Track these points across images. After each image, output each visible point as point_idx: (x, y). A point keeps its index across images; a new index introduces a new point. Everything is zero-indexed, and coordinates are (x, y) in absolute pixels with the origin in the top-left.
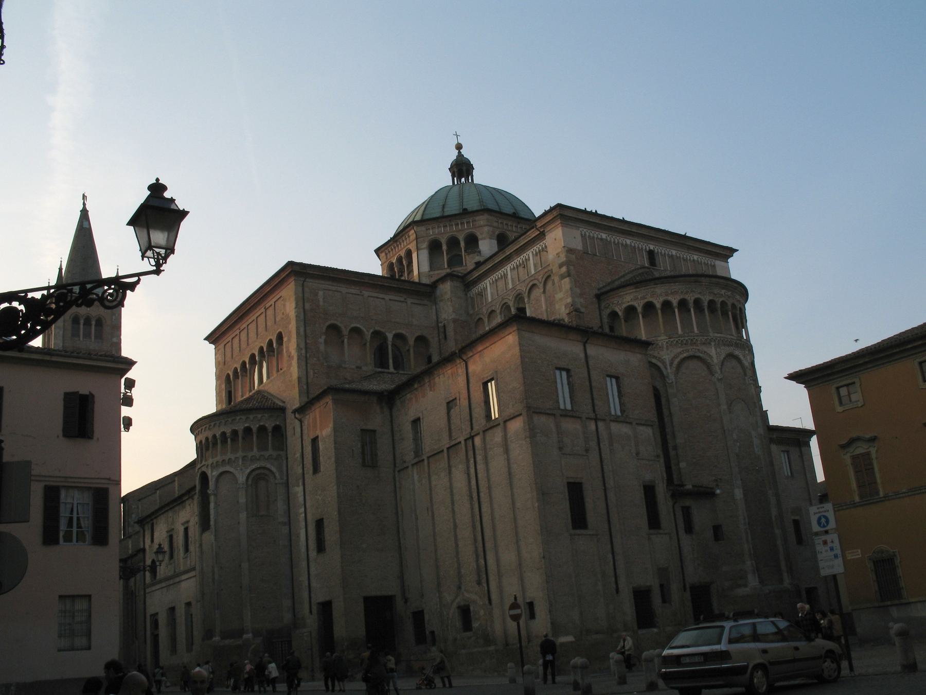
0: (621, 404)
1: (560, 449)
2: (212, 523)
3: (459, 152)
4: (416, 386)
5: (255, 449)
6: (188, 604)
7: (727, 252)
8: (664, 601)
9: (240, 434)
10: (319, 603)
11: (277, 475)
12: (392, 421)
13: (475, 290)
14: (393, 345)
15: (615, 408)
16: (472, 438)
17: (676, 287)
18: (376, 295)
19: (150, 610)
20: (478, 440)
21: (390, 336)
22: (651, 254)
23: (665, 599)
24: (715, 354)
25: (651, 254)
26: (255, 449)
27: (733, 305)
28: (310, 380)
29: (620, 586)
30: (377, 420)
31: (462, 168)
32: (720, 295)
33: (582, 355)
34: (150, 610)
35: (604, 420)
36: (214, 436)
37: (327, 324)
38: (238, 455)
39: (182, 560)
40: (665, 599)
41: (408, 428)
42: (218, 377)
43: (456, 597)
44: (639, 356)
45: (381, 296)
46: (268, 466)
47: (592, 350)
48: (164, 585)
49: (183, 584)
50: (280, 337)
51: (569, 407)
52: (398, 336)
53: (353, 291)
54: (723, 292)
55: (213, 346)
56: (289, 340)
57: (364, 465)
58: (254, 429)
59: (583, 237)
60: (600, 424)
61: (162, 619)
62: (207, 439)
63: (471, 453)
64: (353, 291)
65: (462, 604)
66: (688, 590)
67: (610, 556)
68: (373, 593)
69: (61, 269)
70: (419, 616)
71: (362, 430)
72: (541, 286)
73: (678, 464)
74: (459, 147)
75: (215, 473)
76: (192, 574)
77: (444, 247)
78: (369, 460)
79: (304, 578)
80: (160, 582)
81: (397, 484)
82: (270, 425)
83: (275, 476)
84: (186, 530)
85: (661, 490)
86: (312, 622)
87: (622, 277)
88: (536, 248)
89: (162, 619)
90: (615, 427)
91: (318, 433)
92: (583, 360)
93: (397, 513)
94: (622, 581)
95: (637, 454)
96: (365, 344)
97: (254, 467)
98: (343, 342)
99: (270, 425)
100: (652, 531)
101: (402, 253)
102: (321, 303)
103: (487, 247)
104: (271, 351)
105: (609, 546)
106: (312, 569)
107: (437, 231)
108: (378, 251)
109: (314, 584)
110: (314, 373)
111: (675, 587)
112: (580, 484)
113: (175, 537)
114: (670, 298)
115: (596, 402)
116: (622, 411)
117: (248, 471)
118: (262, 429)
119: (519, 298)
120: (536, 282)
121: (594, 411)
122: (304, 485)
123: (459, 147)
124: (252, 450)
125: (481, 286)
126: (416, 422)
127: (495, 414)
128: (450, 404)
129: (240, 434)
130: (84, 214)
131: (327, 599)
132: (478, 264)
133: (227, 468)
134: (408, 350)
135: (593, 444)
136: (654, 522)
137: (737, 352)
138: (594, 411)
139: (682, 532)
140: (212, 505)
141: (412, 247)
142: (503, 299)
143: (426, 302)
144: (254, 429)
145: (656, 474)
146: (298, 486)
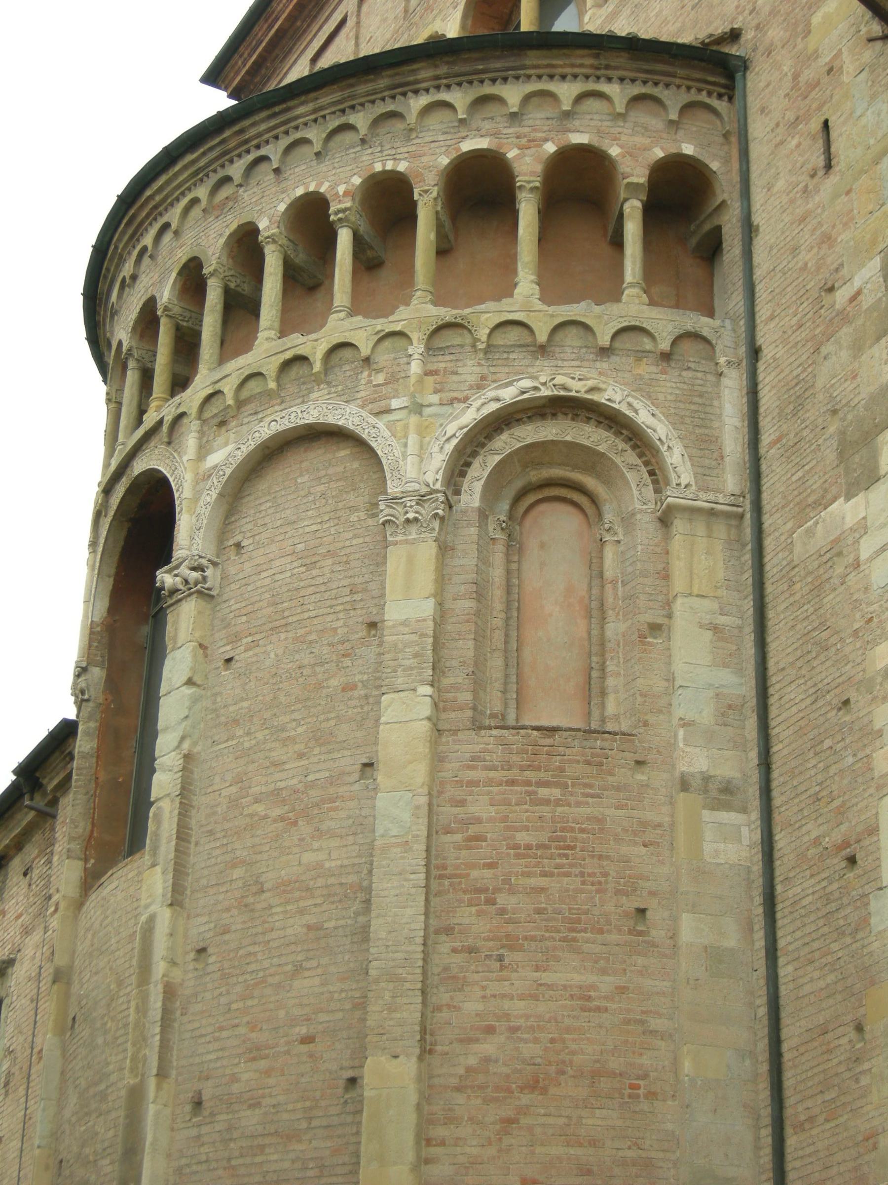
2: (164, 783)
5: (526, 283)
11: (676, 458)
26: (526, 283)
38: (400, 319)
46: (614, 395)
58: (528, 166)
75: (227, 453)
83: (656, 474)
97: (509, 395)
117: (470, 416)
118: (580, 184)
124: (507, 290)
133: (316, 410)
140: (177, 666)
144: (528, 166)
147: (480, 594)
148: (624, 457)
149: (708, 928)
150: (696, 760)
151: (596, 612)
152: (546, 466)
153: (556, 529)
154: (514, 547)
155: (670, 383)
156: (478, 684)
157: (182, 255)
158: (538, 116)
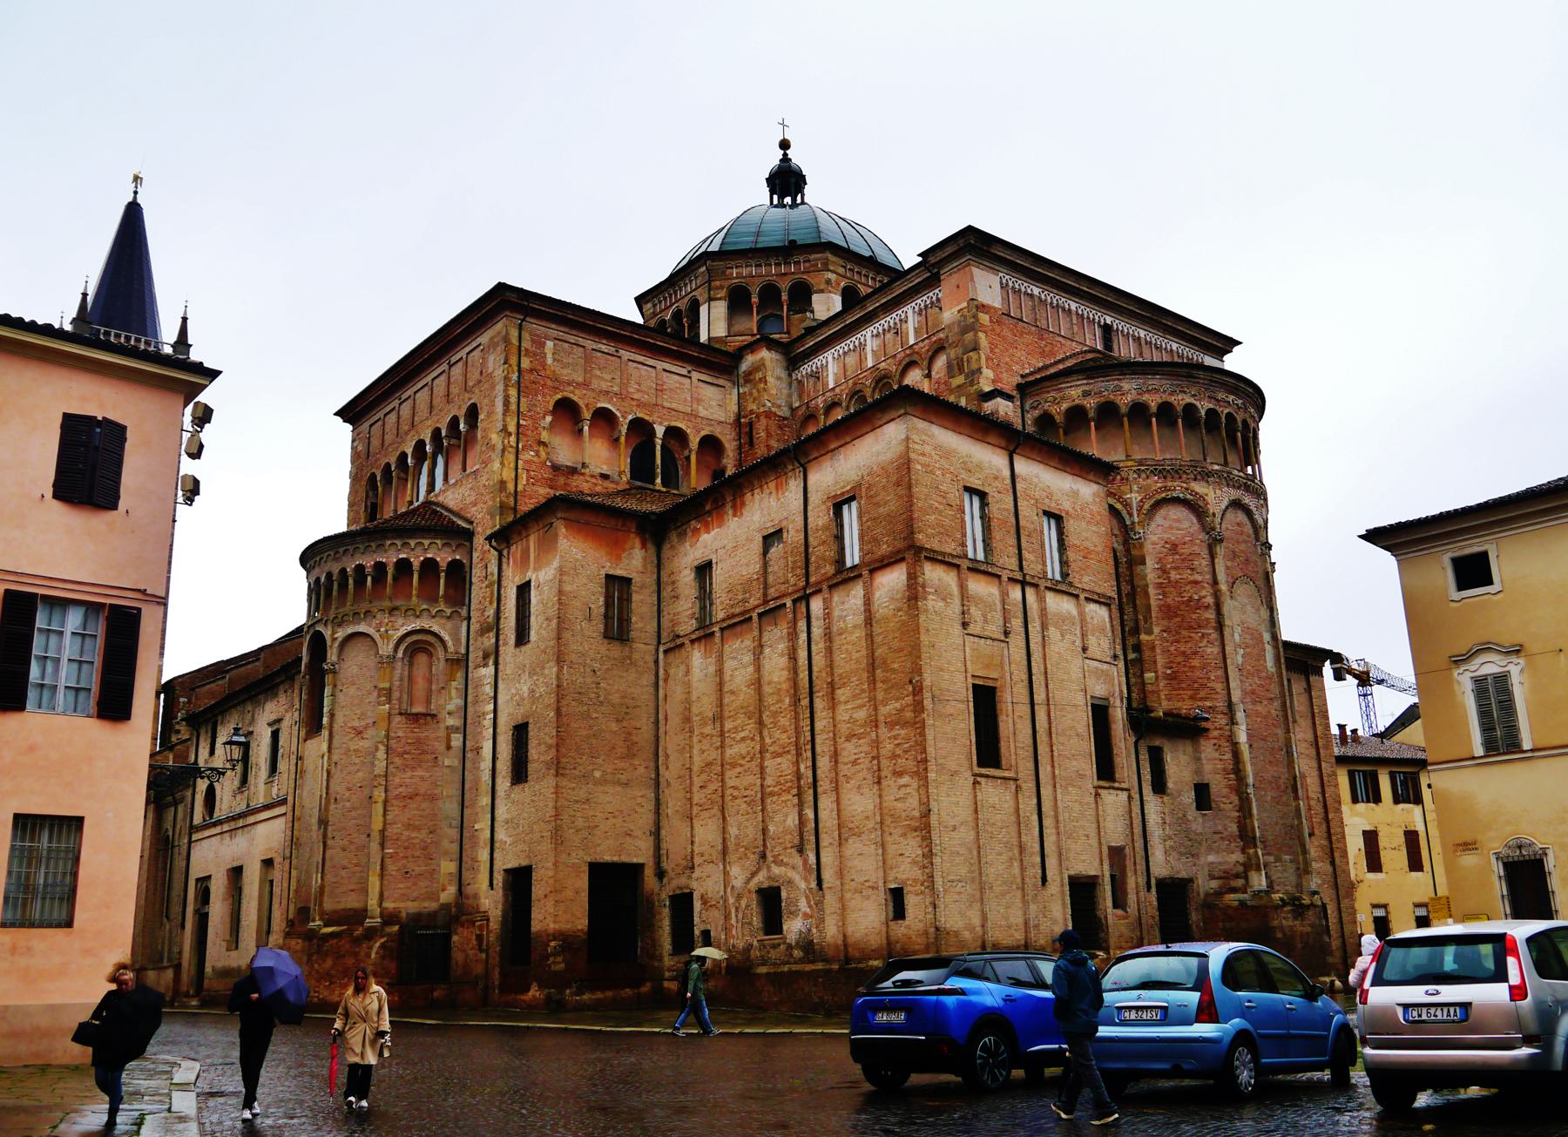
0: (1064, 563)
1: (965, 625)
3: (785, 155)
4: (708, 507)
6: (268, 863)
7: (1226, 344)
8: (1115, 906)
9: (390, 571)
10: (506, 871)
11: (450, 644)
12: (659, 566)
13: (806, 369)
14: (663, 446)
15: (1054, 570)
16: (806, 598)
17: (1154, 382)
18: (641, 359)
19: (196, 872)
20: (816, 605)
21: (660, 431)
22: (1107, 330)
23: (1119, 902)
24: (1216, 497)
25: (1107, 330)
27: (1245, 422)
28: (520, 488)
29: (1049, 874)
30: (634, 561)
31: (786, 181)
32: (1228, 404)
33: (1006, 473)
34: (196, 872)
35: (1036, 586)
36: (343, 571)
37: (559, 396)
39: (262, 787)
40: (1119, 902)
41: (687, 578)
42: (355, 478)
43: (753, 874)
44: (1094, 487)
45: (651, 362)
46: (435, 628)
47: (1023, 466)
48: (226, 827)
49: (260, 827)
50: (473, 413)
51: (981, 556)
52: (674, 433)
53: (604, 348)
54: (1231, 398)
55: (349, 427)
56: (489, 414)
57: (607, 635)
58: (416, 564)
59: (1003, 287)
60: (1030, 592)
61: (218, 887)
63: (802, 625)
64: (604, 348)
65: (765, 885)
66: (1154, 889)
67: (1035, 817)
68: (608, 858)
69: (85, 295)
70: (682, 903)
71: (608, 576)
73: (1142, 676)
74: (785, 145)
75: (340, 634)
76: (281, 810)
77: (755, 299)
78: (617, 627)
79: (483, 825)
80: (220, 822)
81: (661, 672)
82: (444, 557)
84: (275, 736)
85: (1119, 714)
86: (491, 901)
87: (1059, 362)
88: (921, 301)
89: (218, 887)
90: (1052, 600)
91: (531, 575)
92: (1008, 481)
93: (657, 722)
94: (1051, 863)
95: (1084, 649)
96: (617, 440)
98: (581, 431)
99: (444, 557)
100: (1102, 783)
102: (549, 361)
103: (827, 304)
105: (1035, 801)
106: (501, 812)
107: (745, 272)
109: (501, 835)
111: (1133, 881)
112: (993, 689)
113: (253, 745)
114: (1146, 397)
115: (1025, 554)
116: (1065, 575)
118: (430, 566)
120: (916, 358)
121: (1021, 568)
122: (496, 664)
123: (785, 145)
125: (817, 362)
127: (853, 556)
129: (390, 571)
131: (524, 863)
132: (810, 331)
133: (362, 628)
134: (688, 458)
135: (1016, 624)
136: (1106, 769)
137: (1247, 500)
138: (1021, 568)
139: (1147, 789)
141: (701, 294)
142: (855, 384)
143: (721, 382)
144: (416, 564)
145: (1110, 683)
146: (485, 665)
147: (401, 680)
148: (438, 644)
149: (451, 760)
150: (451, 722)
151: (430, 682)
152: (419, 646)
153: (422, 659)
154: (411, 665)
155: (449, 625)
156: (400, 699)
157: (327, 569)
158: (419, 550)
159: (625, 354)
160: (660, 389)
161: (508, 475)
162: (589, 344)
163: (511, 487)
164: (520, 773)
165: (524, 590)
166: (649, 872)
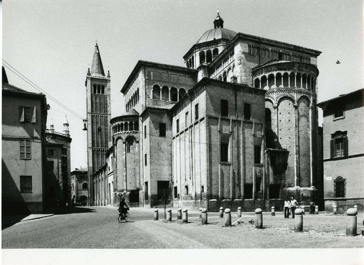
30: (165, 120)
34: (109, 183)
62: (116, 125)
72: (232, 68)
101: (191, 58)
104: (136, 95)
108: (184, 57)
110: (148, 103)
119: (225, 73)
126: (178, 121)
128: (187, 113)
130: (97, 47)
159: (170, 73)
160: (178, 79)
161: (144, 103)
162: (161, 71)
163: (144, 105)
164: (146, 164)
165: (145, 127)
166: (170, 182)
